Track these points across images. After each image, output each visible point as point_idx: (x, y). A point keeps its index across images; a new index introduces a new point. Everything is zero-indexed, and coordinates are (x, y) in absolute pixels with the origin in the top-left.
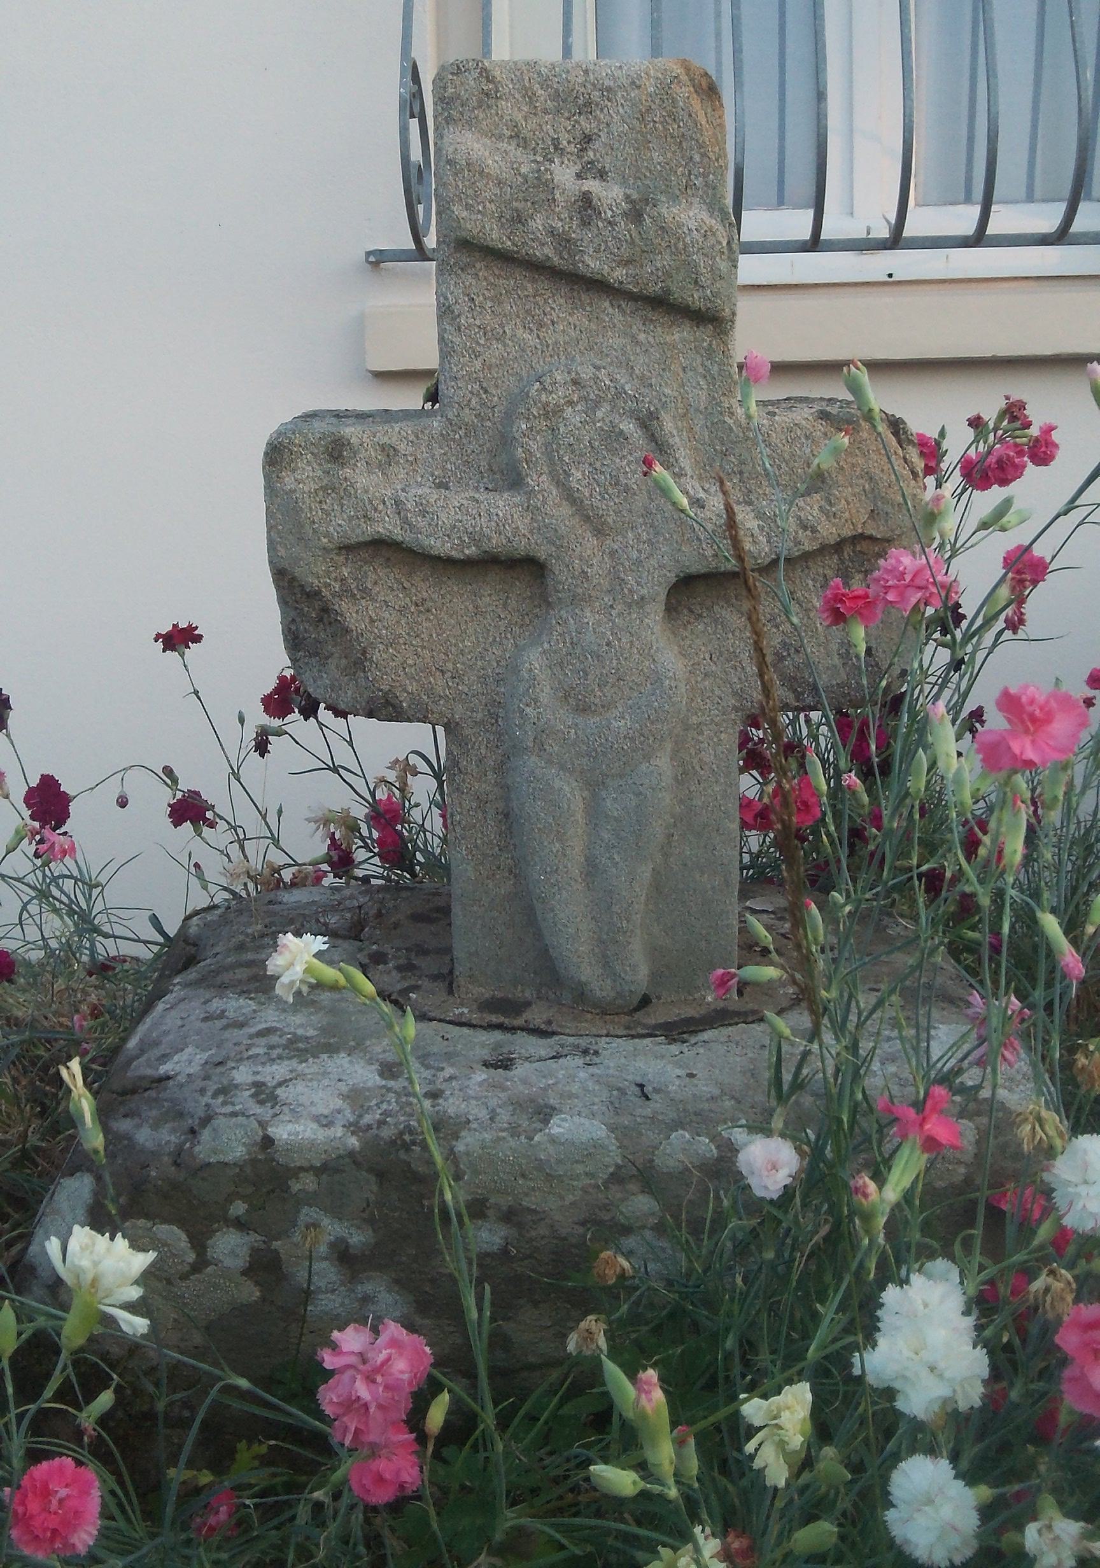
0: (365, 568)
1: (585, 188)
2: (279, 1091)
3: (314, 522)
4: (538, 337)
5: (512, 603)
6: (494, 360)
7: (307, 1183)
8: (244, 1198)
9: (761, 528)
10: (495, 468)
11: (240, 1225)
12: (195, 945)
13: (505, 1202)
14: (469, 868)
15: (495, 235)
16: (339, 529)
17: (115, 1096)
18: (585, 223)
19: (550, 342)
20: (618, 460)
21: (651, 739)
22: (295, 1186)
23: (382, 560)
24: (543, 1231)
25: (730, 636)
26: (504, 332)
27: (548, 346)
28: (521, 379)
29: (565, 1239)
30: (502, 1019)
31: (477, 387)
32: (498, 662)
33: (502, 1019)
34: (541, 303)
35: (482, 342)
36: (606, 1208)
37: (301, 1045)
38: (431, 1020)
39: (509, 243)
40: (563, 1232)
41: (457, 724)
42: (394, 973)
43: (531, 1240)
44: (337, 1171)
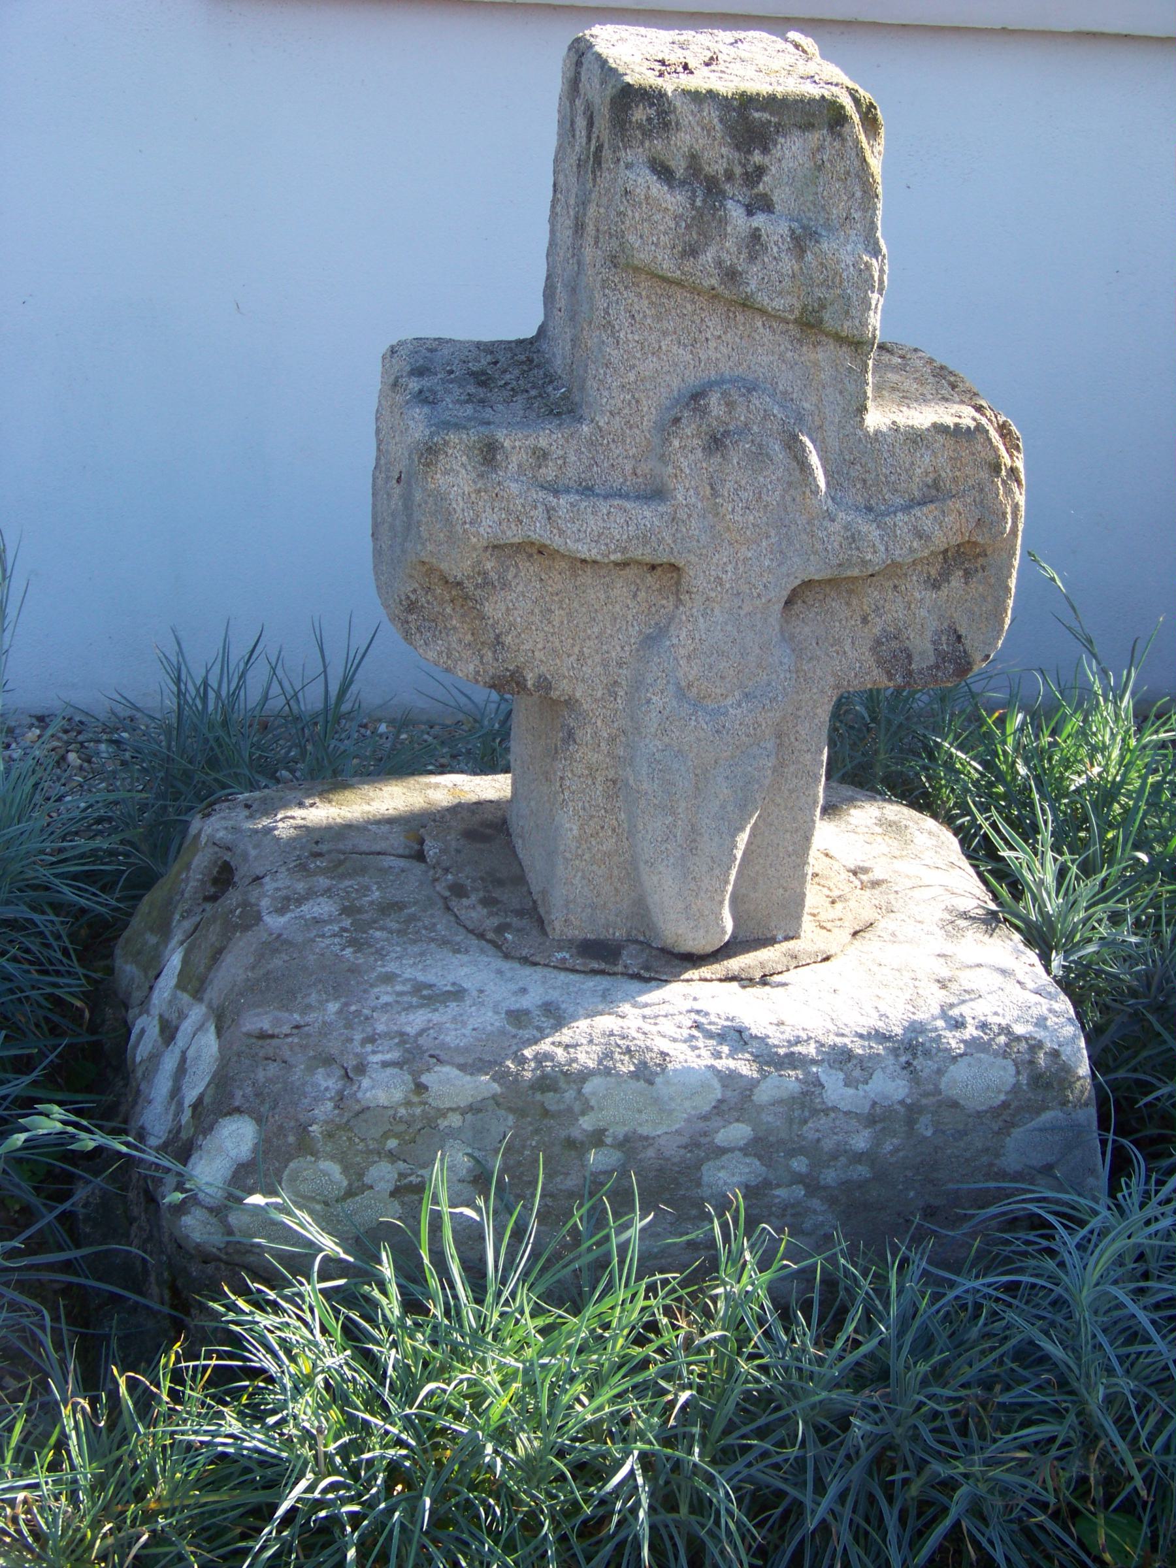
0: (508, 563)
1: (755, 224)
2: (421, 1041)
3: (465, 523)
4: (692, 352)
5: (642, 595)
6: (647, 373)
7: (455, 1120)
8: (397, 1136)
9: (882, 537)
10: (639, 472)
11: (392, 1156)
12: (229, 849)
13: (621, 1131)
14: (575, 827)
15: (674, 288)
16: (489, 530)
17: (254, 1040)
18: (752, 258)
19: (703, 358)
20: (762, 479)
21: (764, 725)
22: (443, 1123)
23: (525, 556)
24: (651, 1152)
25: (837, 624)
26: (660, 347)
27: (700, 362)
28: (672, 391)
29: (668, 1159)
30: (603, 966)
31: (628, 397)
32: (622, 648)
33: (603, 966)
34: (698, 321)
35: (638, 355)
36: (705, 1134)
37: (425, 992)
38: (535, 964)
39: (679, 272)
40: (667, 1154)
41: (577, 701)
42: (479, 908)
43: (640, 1161)
44: (479, 1111)
